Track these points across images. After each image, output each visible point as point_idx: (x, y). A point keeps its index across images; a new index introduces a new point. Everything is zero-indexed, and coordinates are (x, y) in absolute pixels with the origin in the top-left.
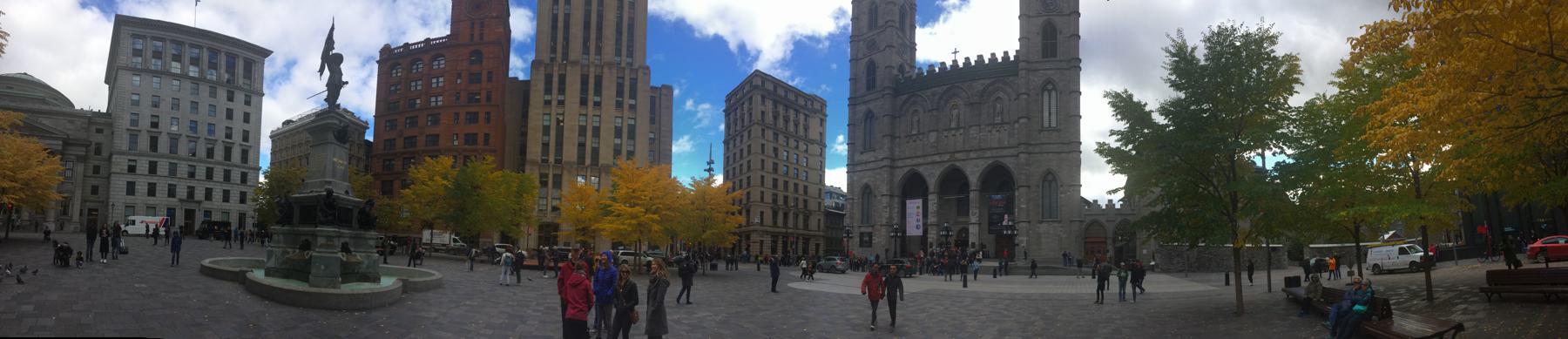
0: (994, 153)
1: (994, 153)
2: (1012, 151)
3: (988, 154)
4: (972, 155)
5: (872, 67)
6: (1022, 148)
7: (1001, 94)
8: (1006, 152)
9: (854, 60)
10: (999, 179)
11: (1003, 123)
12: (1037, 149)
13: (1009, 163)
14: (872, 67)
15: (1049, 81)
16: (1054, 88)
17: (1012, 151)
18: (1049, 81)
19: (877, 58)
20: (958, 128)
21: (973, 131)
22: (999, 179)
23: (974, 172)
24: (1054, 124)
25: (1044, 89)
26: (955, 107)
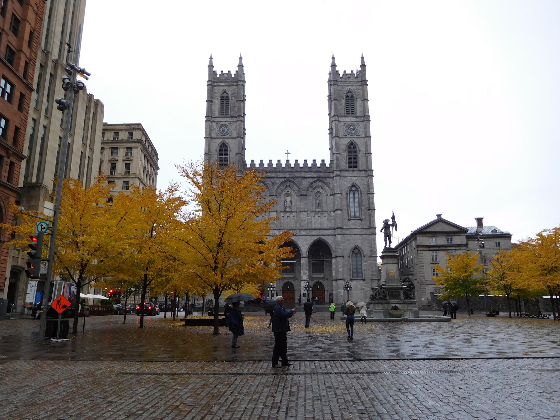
0: (317, 232)
1: (317, 232)
2: (331, 232)
3: (314, 233)
4: (303, 232)
5: (224, 149)
6: (338, 231)
7: (320, 190)
8: (326, 232)
9: (208, 137)
10: (321, 250)
11: (322, 212)
12: (348, 232)
13: (329, 240)
14: (224, 149)
15: (354, 185)
16: (357, 190)
17: (331, 232)
18: (354, 185)
19: (228, 141)
20: (291, 212)
21: (303, 215)
22: (321, 250)
23: (304, 244)
24: (357, 215)
25: (351, 190)
26: (288, 194)
